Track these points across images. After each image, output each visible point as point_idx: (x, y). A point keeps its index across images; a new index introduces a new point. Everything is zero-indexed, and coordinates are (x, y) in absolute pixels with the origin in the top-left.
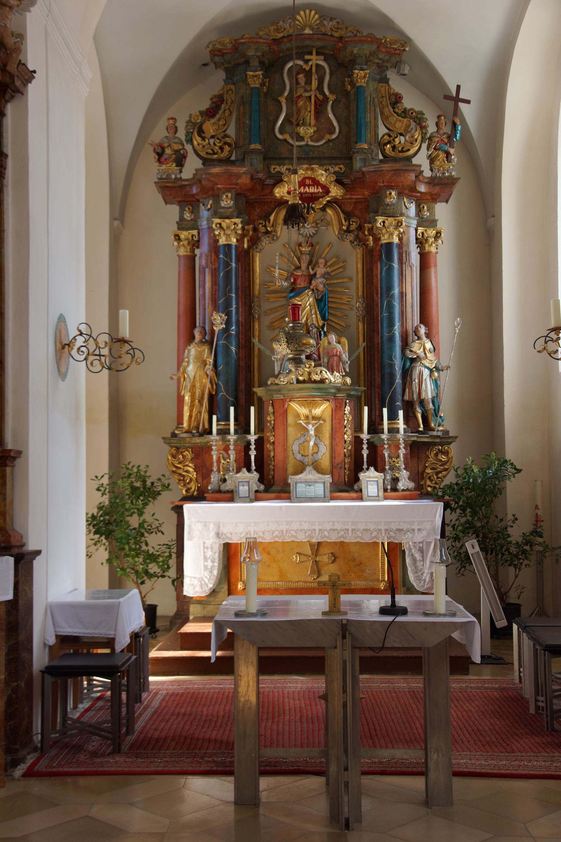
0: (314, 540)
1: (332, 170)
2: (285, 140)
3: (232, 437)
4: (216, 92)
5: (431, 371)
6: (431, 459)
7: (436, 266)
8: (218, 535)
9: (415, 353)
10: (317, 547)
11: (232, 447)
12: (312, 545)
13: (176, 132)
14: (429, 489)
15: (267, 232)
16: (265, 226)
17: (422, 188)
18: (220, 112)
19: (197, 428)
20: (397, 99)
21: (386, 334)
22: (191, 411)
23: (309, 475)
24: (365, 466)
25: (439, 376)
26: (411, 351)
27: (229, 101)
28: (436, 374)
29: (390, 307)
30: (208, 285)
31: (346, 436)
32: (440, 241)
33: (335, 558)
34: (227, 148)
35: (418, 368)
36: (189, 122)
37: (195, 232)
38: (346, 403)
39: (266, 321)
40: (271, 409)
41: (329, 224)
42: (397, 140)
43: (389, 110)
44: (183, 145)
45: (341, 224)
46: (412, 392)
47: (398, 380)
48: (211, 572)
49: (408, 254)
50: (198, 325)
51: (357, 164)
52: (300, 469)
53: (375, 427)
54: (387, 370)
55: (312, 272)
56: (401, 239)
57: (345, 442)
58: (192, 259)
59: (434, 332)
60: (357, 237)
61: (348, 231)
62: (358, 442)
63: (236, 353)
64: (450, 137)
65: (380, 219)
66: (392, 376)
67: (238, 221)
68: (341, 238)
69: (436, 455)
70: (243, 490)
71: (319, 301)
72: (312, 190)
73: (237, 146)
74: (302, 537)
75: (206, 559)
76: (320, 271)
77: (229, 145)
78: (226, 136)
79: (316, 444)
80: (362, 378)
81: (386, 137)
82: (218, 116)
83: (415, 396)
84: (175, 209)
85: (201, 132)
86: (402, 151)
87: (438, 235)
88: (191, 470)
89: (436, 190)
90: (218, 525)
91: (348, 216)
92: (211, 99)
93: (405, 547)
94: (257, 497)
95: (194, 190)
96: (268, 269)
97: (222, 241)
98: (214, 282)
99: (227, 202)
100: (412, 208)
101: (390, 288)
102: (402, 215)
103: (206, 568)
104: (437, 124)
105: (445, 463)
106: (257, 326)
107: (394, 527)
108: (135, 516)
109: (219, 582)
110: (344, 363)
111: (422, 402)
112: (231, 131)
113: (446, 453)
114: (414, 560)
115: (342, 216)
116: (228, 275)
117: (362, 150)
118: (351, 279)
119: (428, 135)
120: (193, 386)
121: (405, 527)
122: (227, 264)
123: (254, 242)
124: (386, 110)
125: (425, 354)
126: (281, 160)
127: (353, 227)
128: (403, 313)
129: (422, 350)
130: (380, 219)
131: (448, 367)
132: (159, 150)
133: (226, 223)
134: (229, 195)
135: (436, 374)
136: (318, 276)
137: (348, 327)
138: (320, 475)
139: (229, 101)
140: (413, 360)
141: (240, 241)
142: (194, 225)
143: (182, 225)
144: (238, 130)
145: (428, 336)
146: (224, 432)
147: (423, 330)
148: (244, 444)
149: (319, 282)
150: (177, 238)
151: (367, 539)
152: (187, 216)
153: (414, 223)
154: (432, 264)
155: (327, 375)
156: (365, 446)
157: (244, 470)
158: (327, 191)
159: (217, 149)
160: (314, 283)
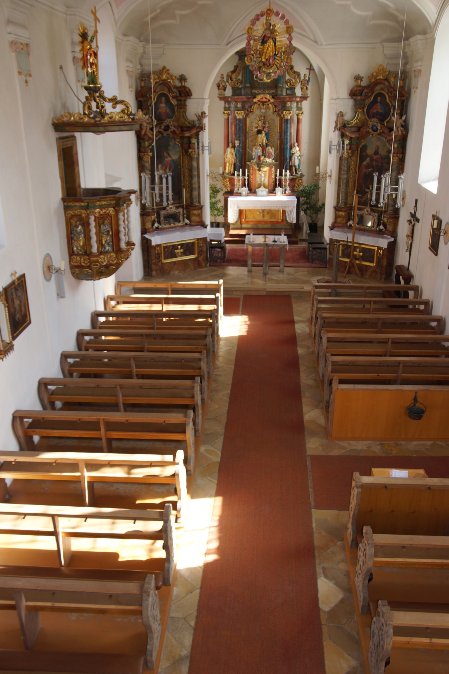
0: (263, 209)
1: (271, 92)
2: (257, 81)
3: (241, 178)
4: (235, 64)
5: (298, 157)
6: (297, 182)
7: (301, 122)
8: (238, 207)
10: (263, 211)
11: (241, 180)
12: (262, 210)
13: (223, 78)
14: (296, 190)
15: (251, 112)
16: (250, 109)
17: (298, 99)
18: (237, 71)
19: (230, 173)
20: (292, 67)
22: (229, 168)
23: (262, 188)
24: (277, 186)
25: (300, 158)
27: (240, 67)
28: (299, 158)
29: (287, 138)
30: (233, 128)
32: (303, 115)
33: (268, 213)
34: (239, 84)
36: (227, 75)
37: (229, 111)
39: (250, 139)
40: (251, 168)
41: (270, 109)
42: (291, 82)
43: (289, 71)
44: (225, 83)
45: (273, 109)
47: (288, 160)
48: (236, 217)
49: (293, 120)
50: (230, 141)
51: (279, 92)
52: (259, 187)
53: (281, 174)
54: (285, 157)
55: (264, 126)
56: (291, 117)
58: (228, 119)
60: (278, 114)
61: (276, 111)
62: (276, 179)
63: (242, 151)
64: (308, 81)
65: (284, 112)
66: (286, 159)
67: (243, 112)
68: (273, 114)
69: (299, 180)
70: (244, 193)
71: (266, 134)
72: (265, 100)
73: (241, 83)
74: (260, 208)
75: (234, 213)
76: (267, 125)
77: (240, 83)
78: (239, 80)
79: (264, 179)
81: (288, 81)
82: (236, 73)
83: (293, 164)
84: (222, 102)
85: (231, 78)
86: (293, 85)
87: (302, 113)
88: (228, 184)
89: (302, 99)
90: (238, 205)
91: (276, 107)
92: (234, 67)
93: (286, 211)
94: (247, 195)
95: (230, 99)
96: (251, 123)
97: (238, 117)
98: (235, 128)
99: (239, 105)
100: (295, 104)
101: (287, 133)
102: (291, 108)
103: (234, 216)
104: (304, 77)
105: (300, 183)
106: (247, 141)
107: (284, 206)
108: (214, 199)
109: (238, 219)
110: (273, 155)
111: (295, 166)
112: (240, 77)
113: (301, 180)
114: (289, 214)
115: (274, 106)
116: (239, 128)
117: (280, 87)
118: (276, 127)
119: (301, 80)
120: (229, 161)
121: (286, 206)
122: (239, 125)
123: (247, 115)
124: (288, 71)
126: (255, 89)
127: (277, 110)
128: (290, 139)
130: (284, 112)
131: (303, 156)
132: (218, 85)
133: (239, 112)
134: (240, 103)
136: (266, 127)
137: (274, 141)
138: (265, 189)
139: (240, 67)
140: (293, 154)
141: (243, 116)
142: (228, 109)
143: (225, 109)
144: (242, 77)
145: (298, 146)
146: (238, 175)
147: (296, 144)
148: (243, 180)
149: (266, 129)
150: (224, 113)
151: (276, 209)
152: (227, 106)
153: (295, 109)
154: (300, 122)
155: (268, 160)
156: (278, 181)
157: (244, 187)
158: (269, 101)
159: (236, 84)
160: (265, 129)
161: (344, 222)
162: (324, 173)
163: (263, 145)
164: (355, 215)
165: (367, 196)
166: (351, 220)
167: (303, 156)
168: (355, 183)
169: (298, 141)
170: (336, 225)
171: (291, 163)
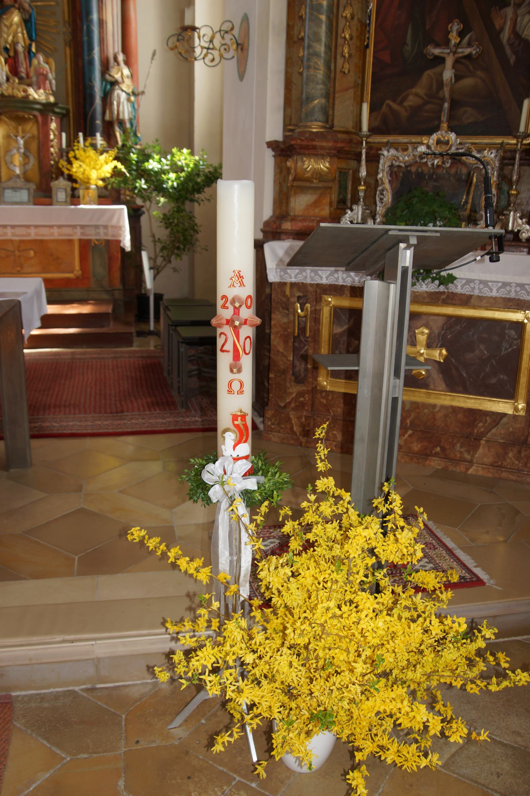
5: (128, 94)
9: (113, 77)
14: (128, 198)
21: (86, 58)
26: (110, 75)
29: (90, 32)
31: (52, 150)
35: (117, 92)
38: (52, 120)
46: (111, 112)
47: (98, 101)
57: (52, 154)
59: (133, 60)
66: (92, 97)
80: (70, 99)
111: (121, 123)
125: (123, 79)
128: (102, 41)
129: (120, 74)
131: (143, 93)
135: (132, 98)
145: (127, 63)
147: (121, 57)
155: (31, 91)
161: (326, 211)
162: (216, 29)
163: (16, 52)
164: (383, 175)
165: (441, 74)
166: (355, 200)
167: (143, 93)
168: (364, 26)
169: (125, 48)
170: (287, 226)
171: (108, 112)
